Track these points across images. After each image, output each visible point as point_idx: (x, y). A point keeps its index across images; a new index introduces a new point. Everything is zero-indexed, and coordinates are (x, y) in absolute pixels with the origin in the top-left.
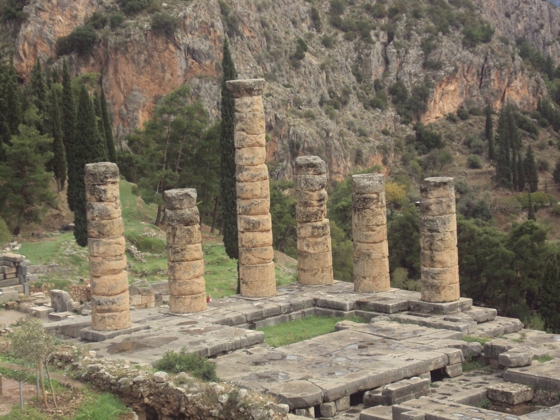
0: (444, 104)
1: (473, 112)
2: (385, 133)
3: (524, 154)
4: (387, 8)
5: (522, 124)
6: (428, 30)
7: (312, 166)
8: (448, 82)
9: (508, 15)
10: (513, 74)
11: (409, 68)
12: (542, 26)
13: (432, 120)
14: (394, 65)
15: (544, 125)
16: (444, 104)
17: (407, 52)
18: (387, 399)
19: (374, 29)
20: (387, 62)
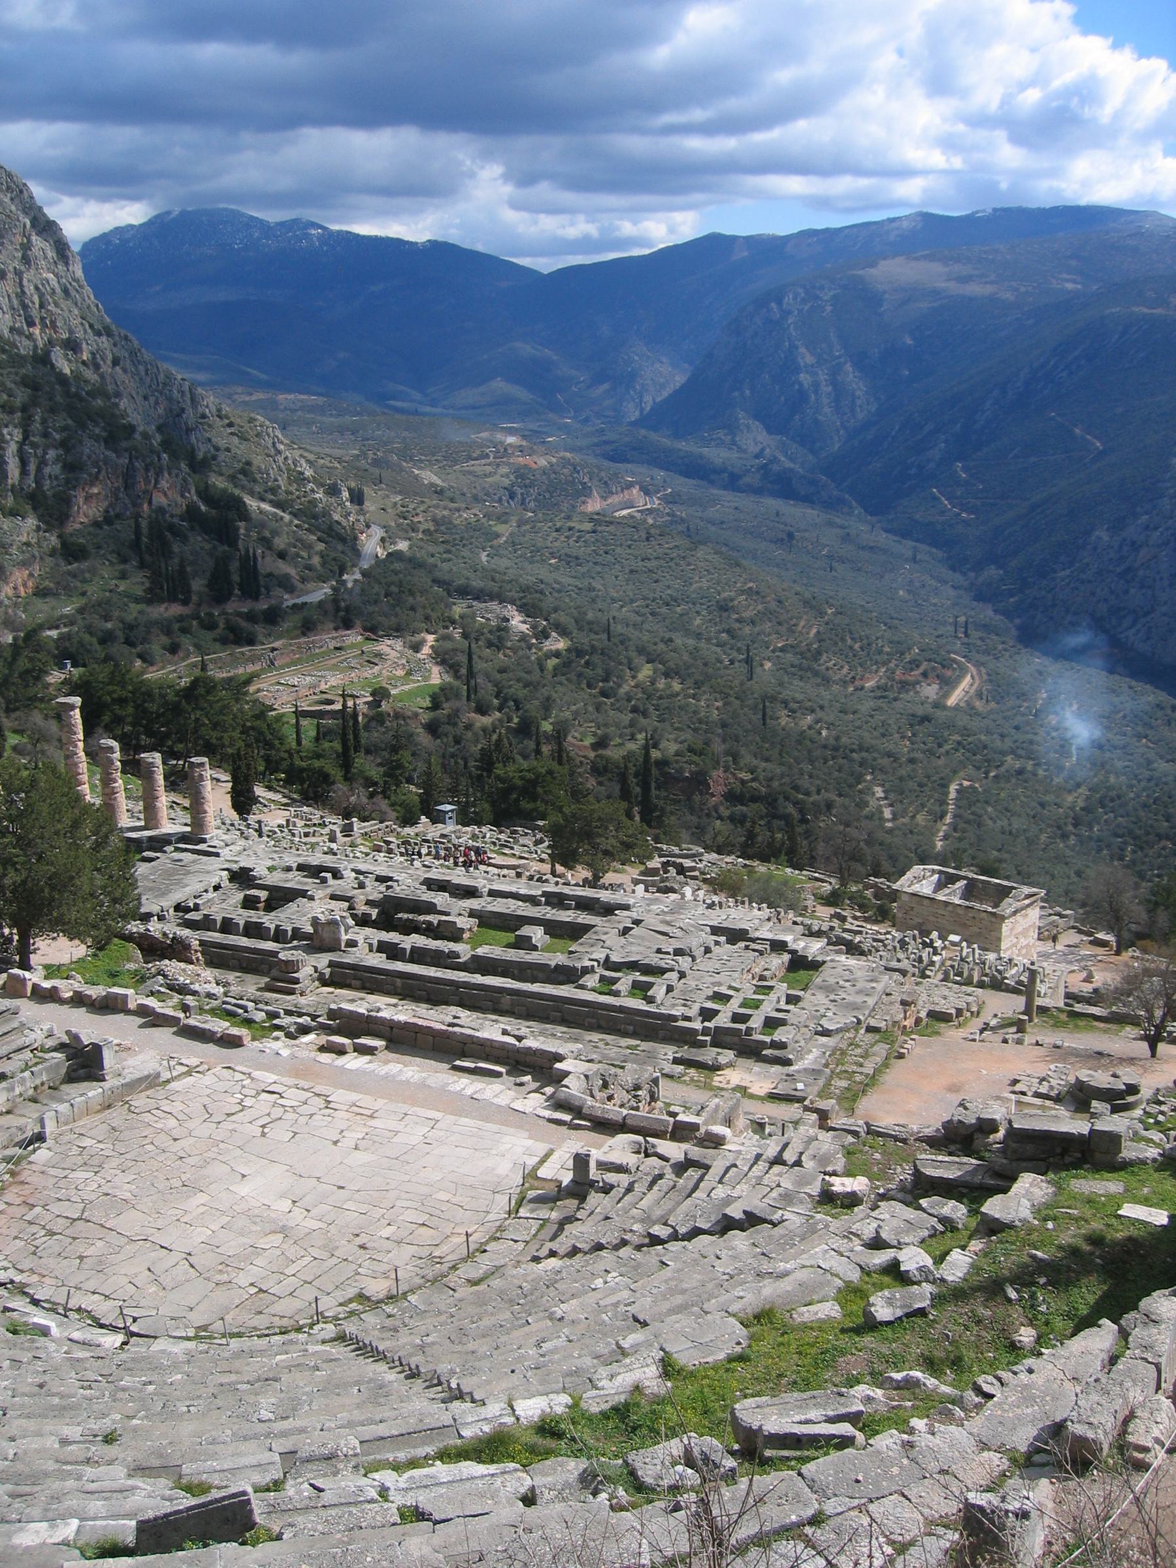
0: (86, 510)
1: (118, 516)
2: (28, 544)
3: (176, 560)
4: (18, 402)
5: (171, 528)
6: (64, 429)
7: (112, 748)
8: (92, 485)
9: (146, 398)
10: (159, 474)
11: (47, 470)
12: (183, 410)
13: (78, 526)
14: (32, 467)
15: (192, 529)
16: (86, 510)
17: (45, 453)
18: (196, 908)
19: (6, 426)
20: (24, 463)
